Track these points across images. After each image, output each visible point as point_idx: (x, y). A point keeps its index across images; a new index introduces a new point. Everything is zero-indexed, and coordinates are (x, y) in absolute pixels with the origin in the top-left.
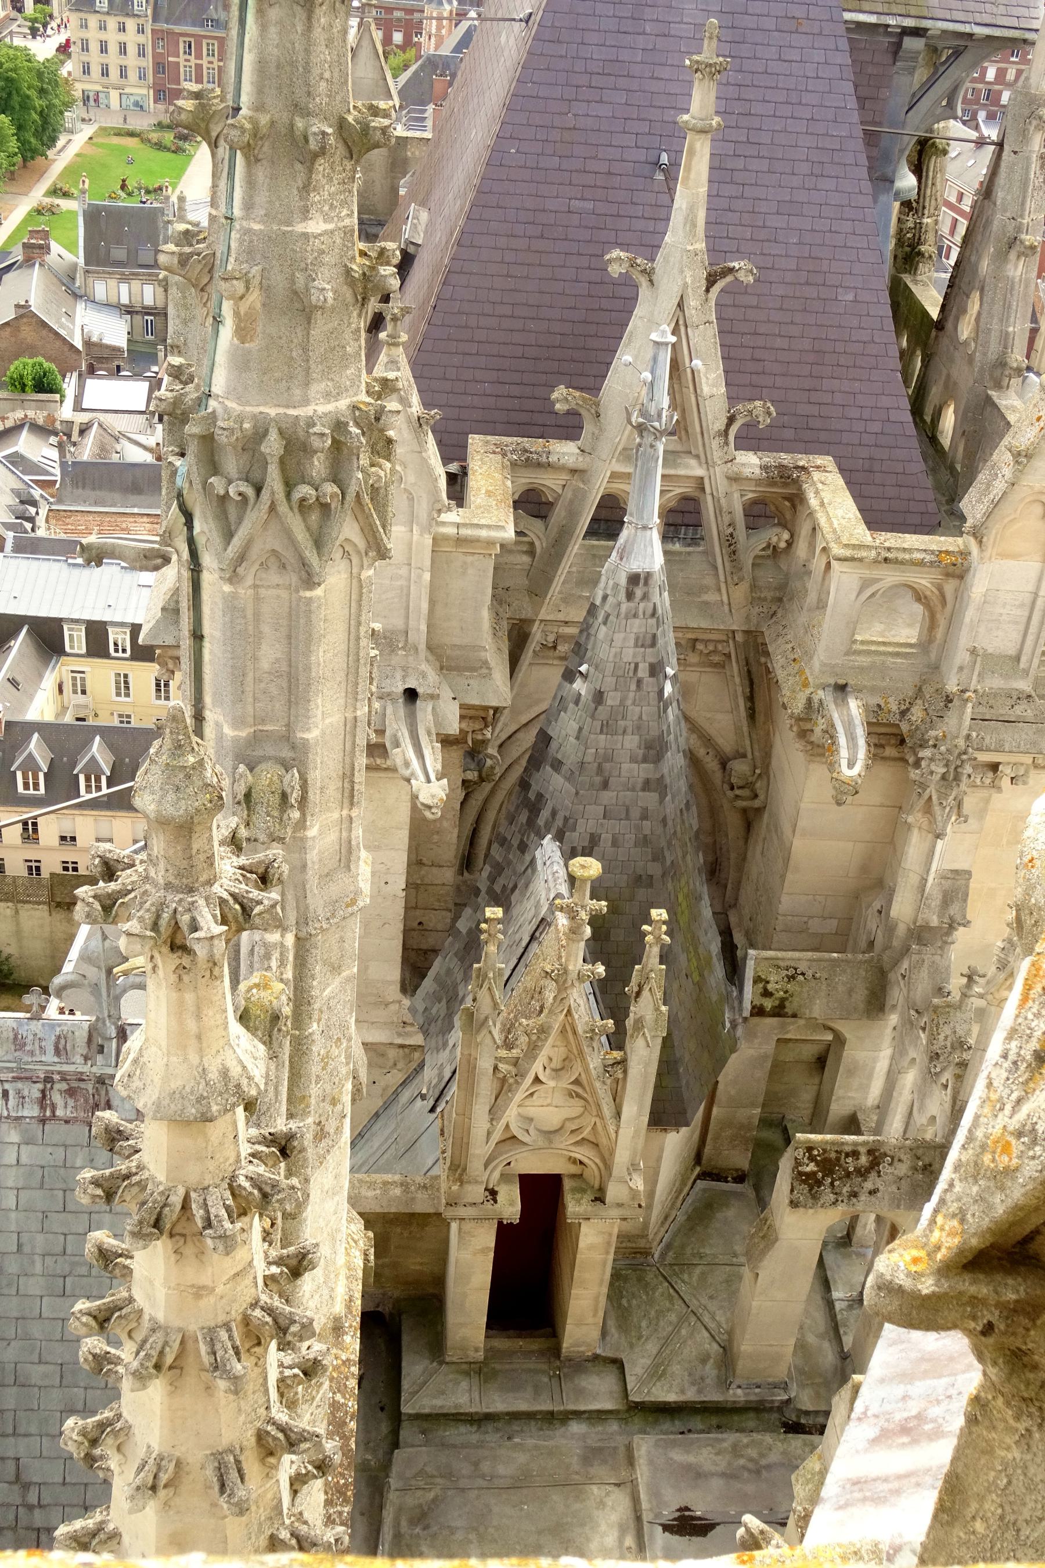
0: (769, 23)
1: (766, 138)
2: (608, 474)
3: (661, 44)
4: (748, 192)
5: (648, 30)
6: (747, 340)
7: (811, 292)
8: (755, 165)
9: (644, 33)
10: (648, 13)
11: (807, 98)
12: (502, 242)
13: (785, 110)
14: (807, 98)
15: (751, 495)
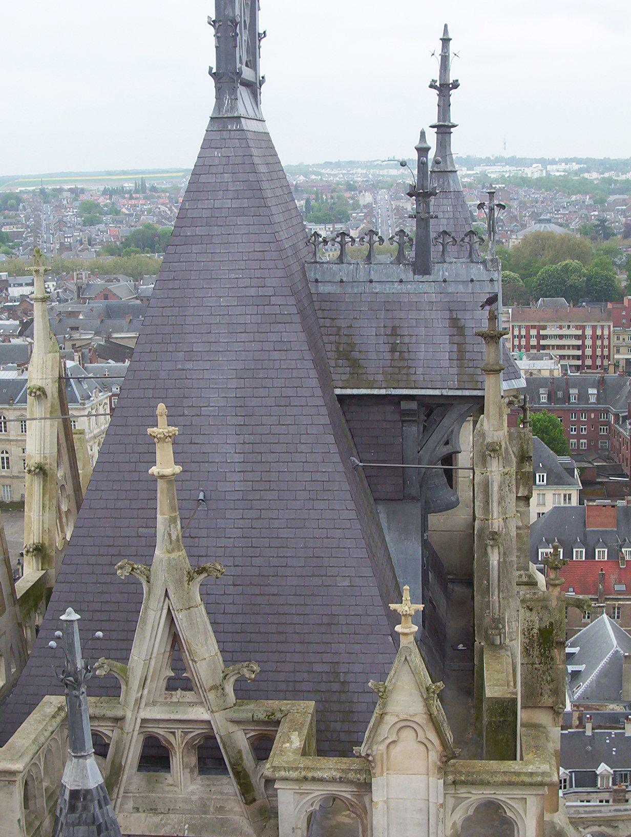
0: (271, 402)
1: (274, 476)
2: (139, 721)
3: (195, 420)
4: (264, 514)
5: (186, 412)
6: (270, 619)
7: (317, 581)
8: (269, 495)
9: (183, 415)
10: (186, 402)
11: (302, 448)
12: (93, 560)
13: (286, 457)
14: (302, 448)
15: (253, 734)
